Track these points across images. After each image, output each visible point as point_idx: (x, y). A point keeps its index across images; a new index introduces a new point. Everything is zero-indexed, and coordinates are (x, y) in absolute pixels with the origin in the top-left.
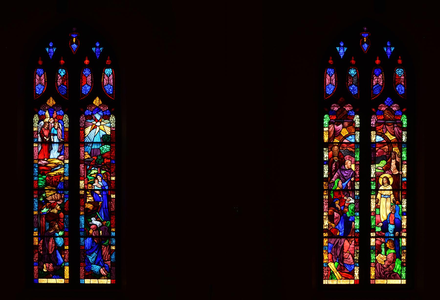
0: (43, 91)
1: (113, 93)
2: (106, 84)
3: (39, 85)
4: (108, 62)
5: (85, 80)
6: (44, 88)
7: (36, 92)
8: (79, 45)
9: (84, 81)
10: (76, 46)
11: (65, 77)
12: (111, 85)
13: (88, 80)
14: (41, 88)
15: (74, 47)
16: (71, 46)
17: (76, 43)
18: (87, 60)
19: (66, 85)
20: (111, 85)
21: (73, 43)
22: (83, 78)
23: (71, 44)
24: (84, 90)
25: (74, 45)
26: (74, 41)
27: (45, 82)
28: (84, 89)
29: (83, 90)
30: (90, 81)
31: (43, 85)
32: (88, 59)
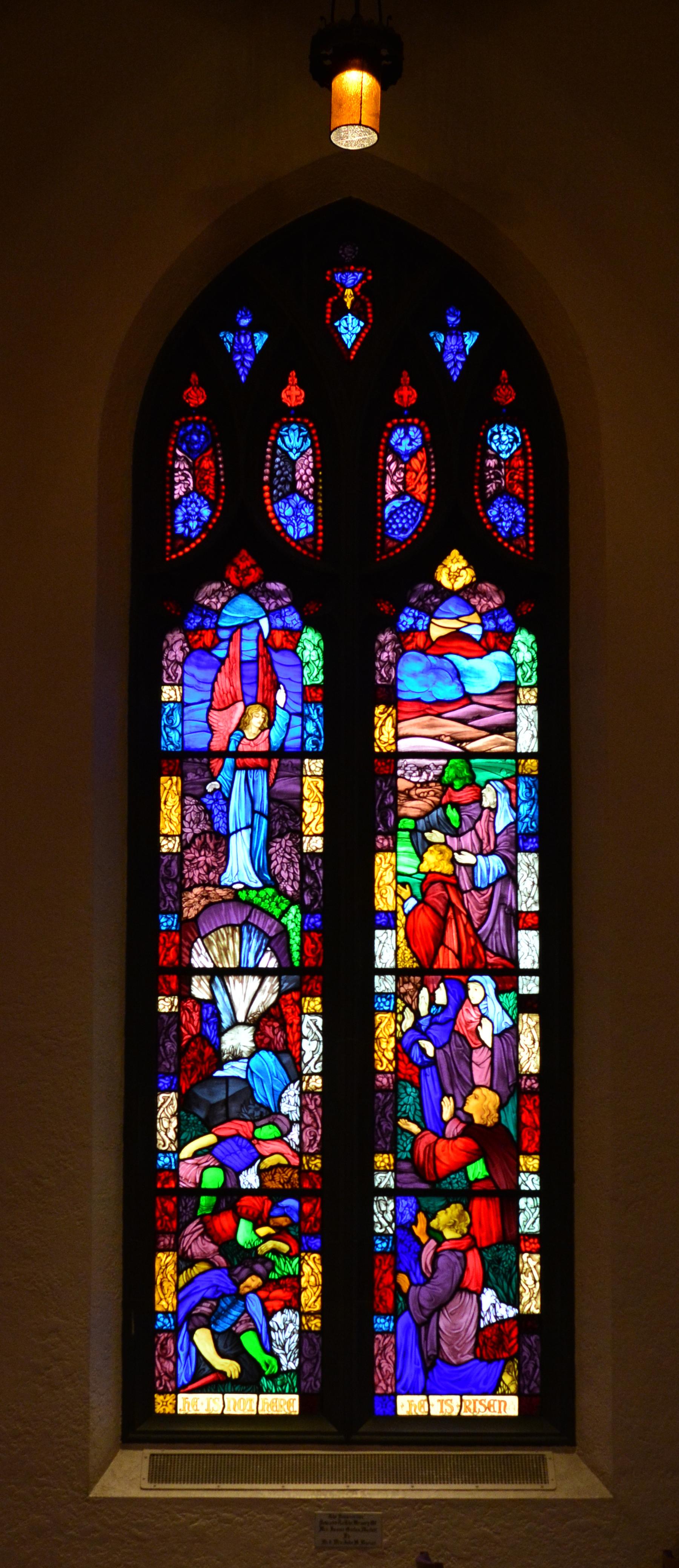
4: (506, 395)
8: (371, 321)
10: (359, 325)
15: (347, 328)
18: (405, 388)
21: (340, 311)
23: (332, 314)
25: (350, 321)
26: (349, 301)
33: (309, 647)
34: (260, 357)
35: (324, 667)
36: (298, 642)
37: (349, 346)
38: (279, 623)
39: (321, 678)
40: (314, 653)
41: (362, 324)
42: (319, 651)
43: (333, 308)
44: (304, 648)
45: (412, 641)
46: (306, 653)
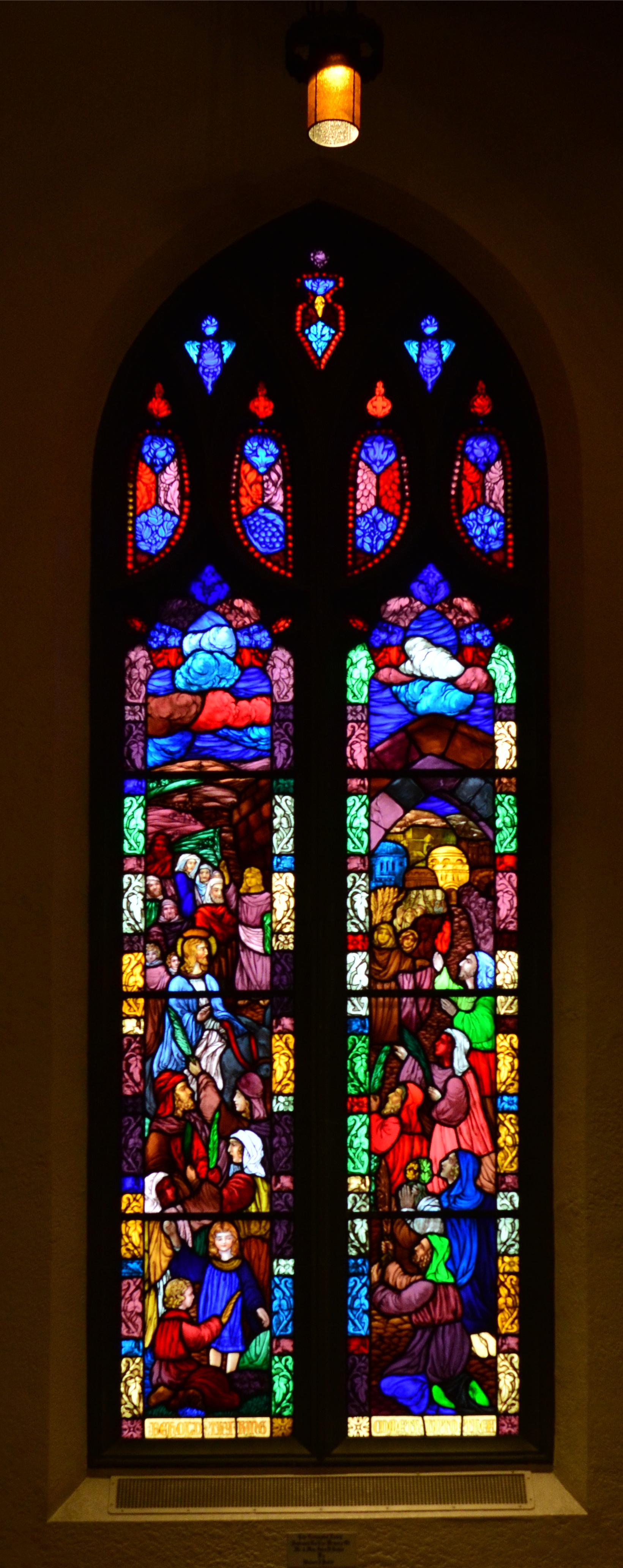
0: (169, 539)
1: (503, 548)
2: (474, 505)
3: (151, 509)
5: (369, 487)
6: (177, 527)
7: (135, 542)
8: (342, 329)
9: (366, 494)
11: (274, 476)
12: (496, 510)
13: (386, 487)
14: (162, 524)
16: (303, 330)
17: (329, 319)
19: (281, 509)
20: (496, 510)
21: (311, 319)
22: (359, 480)
23: (303, 321)
24: (364, 536)
27: (182, 496)
28: (364, 531)
29: (359, 532)
30: (393, 491)
31: (173, 514)
32: (387, 395)
33: (279, 664)
34: (226, 367)
35: (294, 686)
36: (268, 659)
37: (319, 353)
38: (245, 640)
39: (291, 695)
40: (284, 671)
41: (333, 332)
42: (290, 670)
43: (302, 316)
44: (274, 667)
45: (384, 657)
46: (276, 672)
